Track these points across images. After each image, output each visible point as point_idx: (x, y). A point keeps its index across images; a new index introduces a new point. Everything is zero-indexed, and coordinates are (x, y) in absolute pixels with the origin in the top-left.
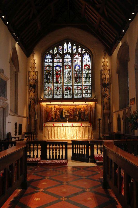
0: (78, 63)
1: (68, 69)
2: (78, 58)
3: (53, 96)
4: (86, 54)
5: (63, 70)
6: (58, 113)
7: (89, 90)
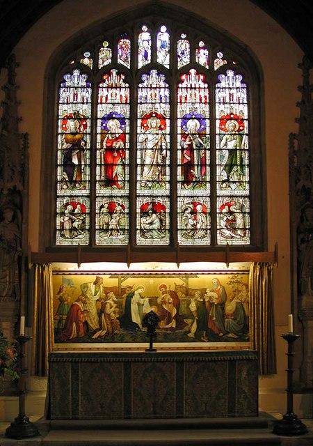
0: (197, 105)
1: (154, 131)
2: (195, 88)
3: (92, 238)
4: (230, 73)
5: (133, 134)
6: (112, 309)
7: (239, 217)
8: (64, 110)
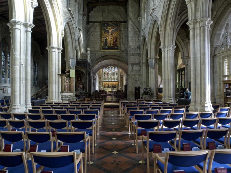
6: (108, 86)
8: (104, 70)
